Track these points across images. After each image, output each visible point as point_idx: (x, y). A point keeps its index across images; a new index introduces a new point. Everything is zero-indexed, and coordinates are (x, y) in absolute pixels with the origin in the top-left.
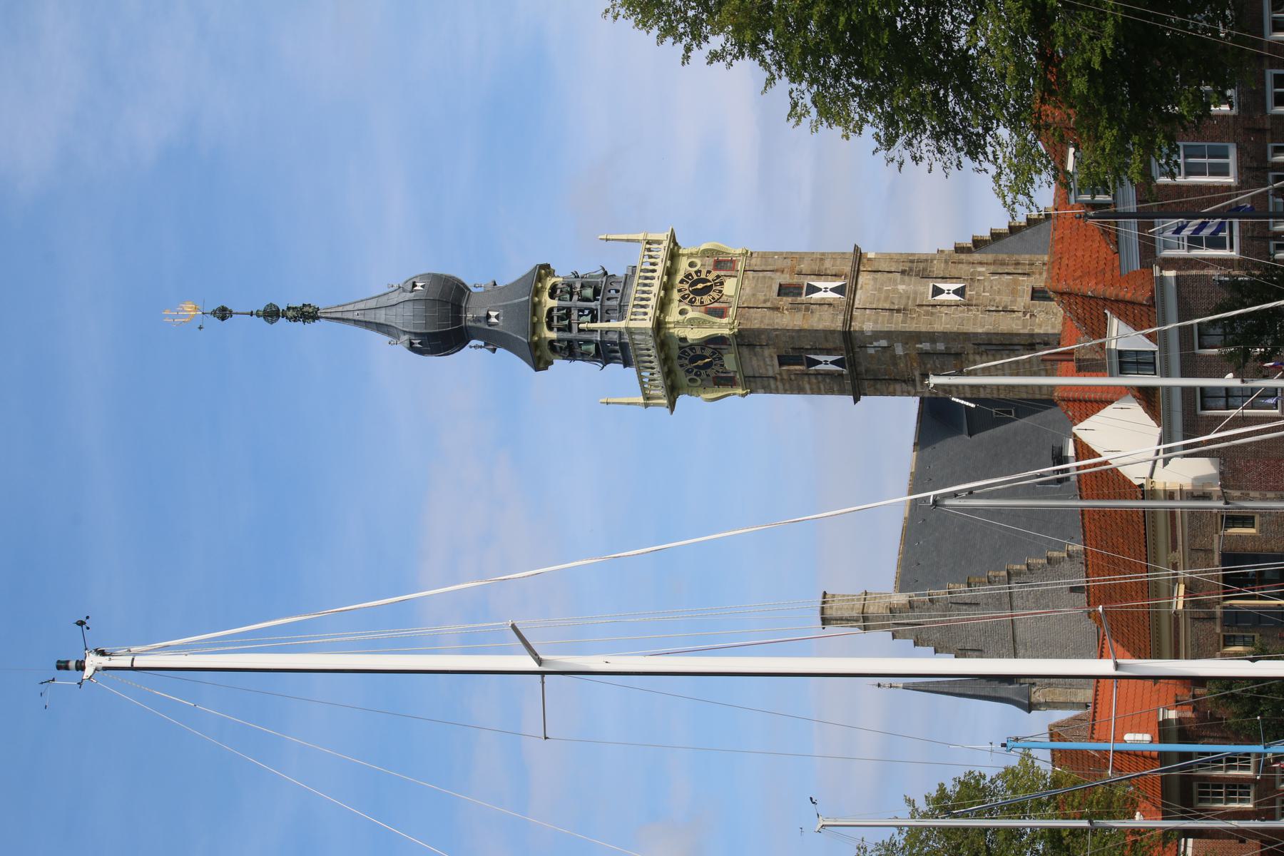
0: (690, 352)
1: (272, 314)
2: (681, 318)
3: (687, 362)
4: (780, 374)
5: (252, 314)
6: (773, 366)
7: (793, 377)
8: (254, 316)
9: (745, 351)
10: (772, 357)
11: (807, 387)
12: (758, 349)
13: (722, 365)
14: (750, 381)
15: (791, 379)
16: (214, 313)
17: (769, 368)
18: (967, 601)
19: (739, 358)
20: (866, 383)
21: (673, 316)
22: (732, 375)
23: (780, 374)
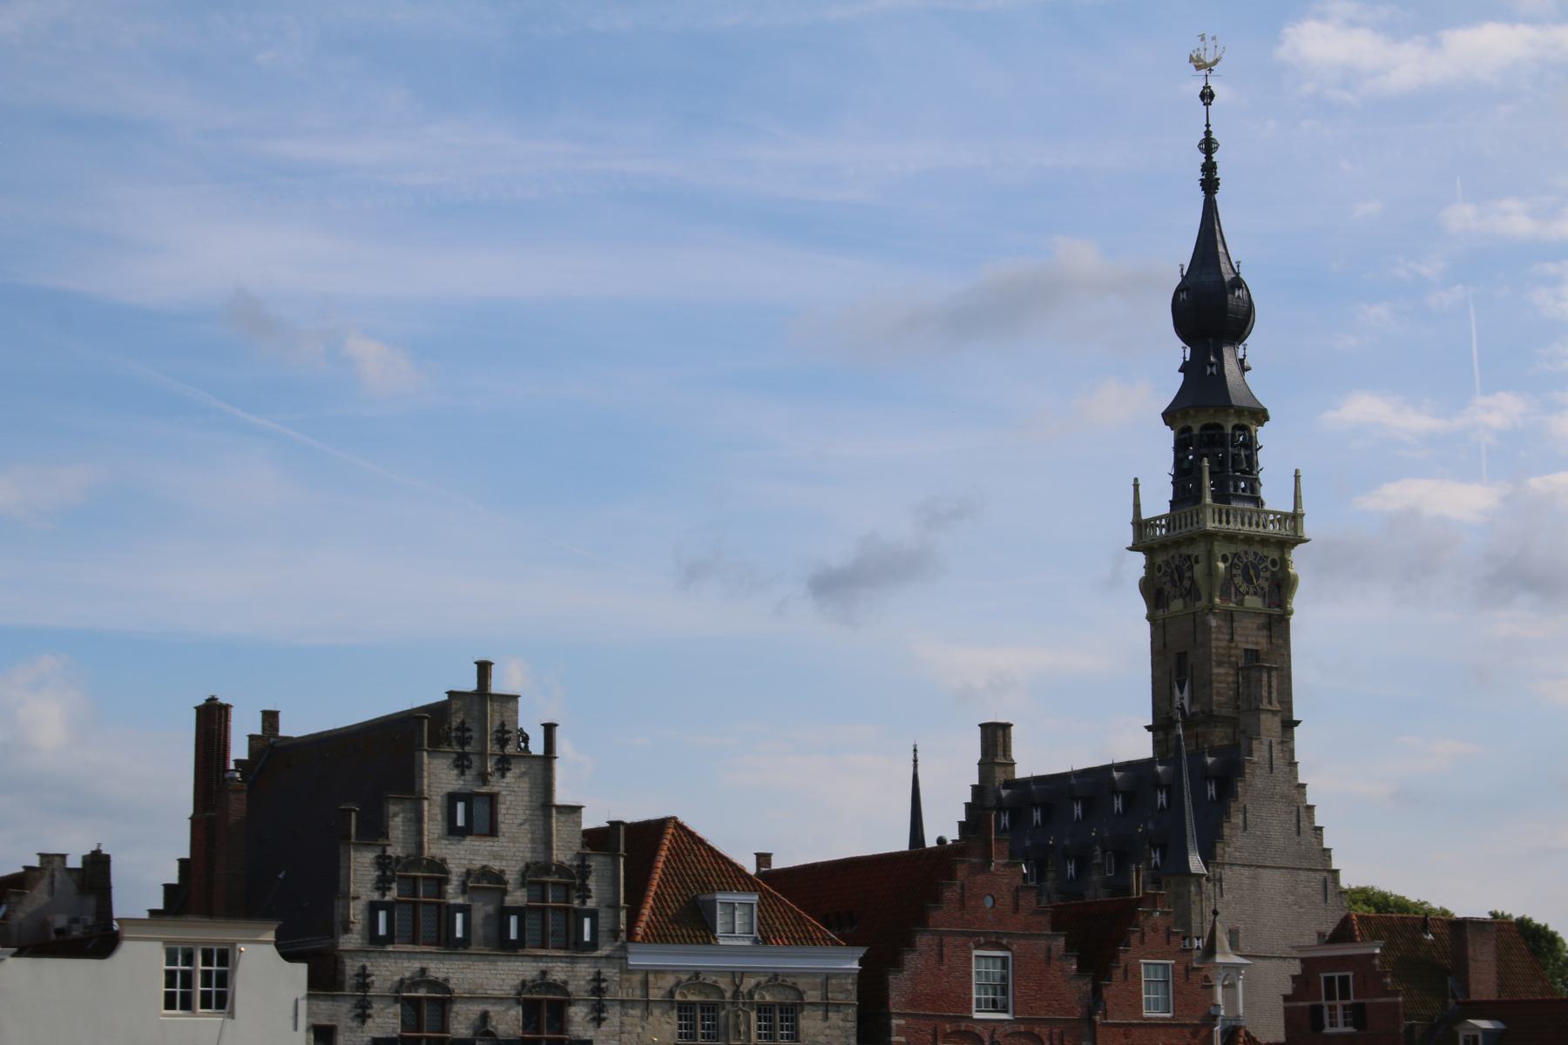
0: (1263, 565)
1: (1208, 145)
2: (1219, 556)
3: (1251, 559)
4: (1236, 647)
5: (1208, 125)
6: (1247, 642)
7: (1233, 659)
8: (1205, 129)
9: (1261, 620)
10: (1257, 644)
11: (1221, 670)
12: (1265, 633)
13: (1248, 593)
14: (1226, 615)
15: (1230, 656)
16: (1207, 87)
17: (1244, 639)
18: (1301, 823)
19: (1255, 613)
20: (1230, 730)
21: (1220, 549)
22: (1233, 599)
23: (1236, 647)
